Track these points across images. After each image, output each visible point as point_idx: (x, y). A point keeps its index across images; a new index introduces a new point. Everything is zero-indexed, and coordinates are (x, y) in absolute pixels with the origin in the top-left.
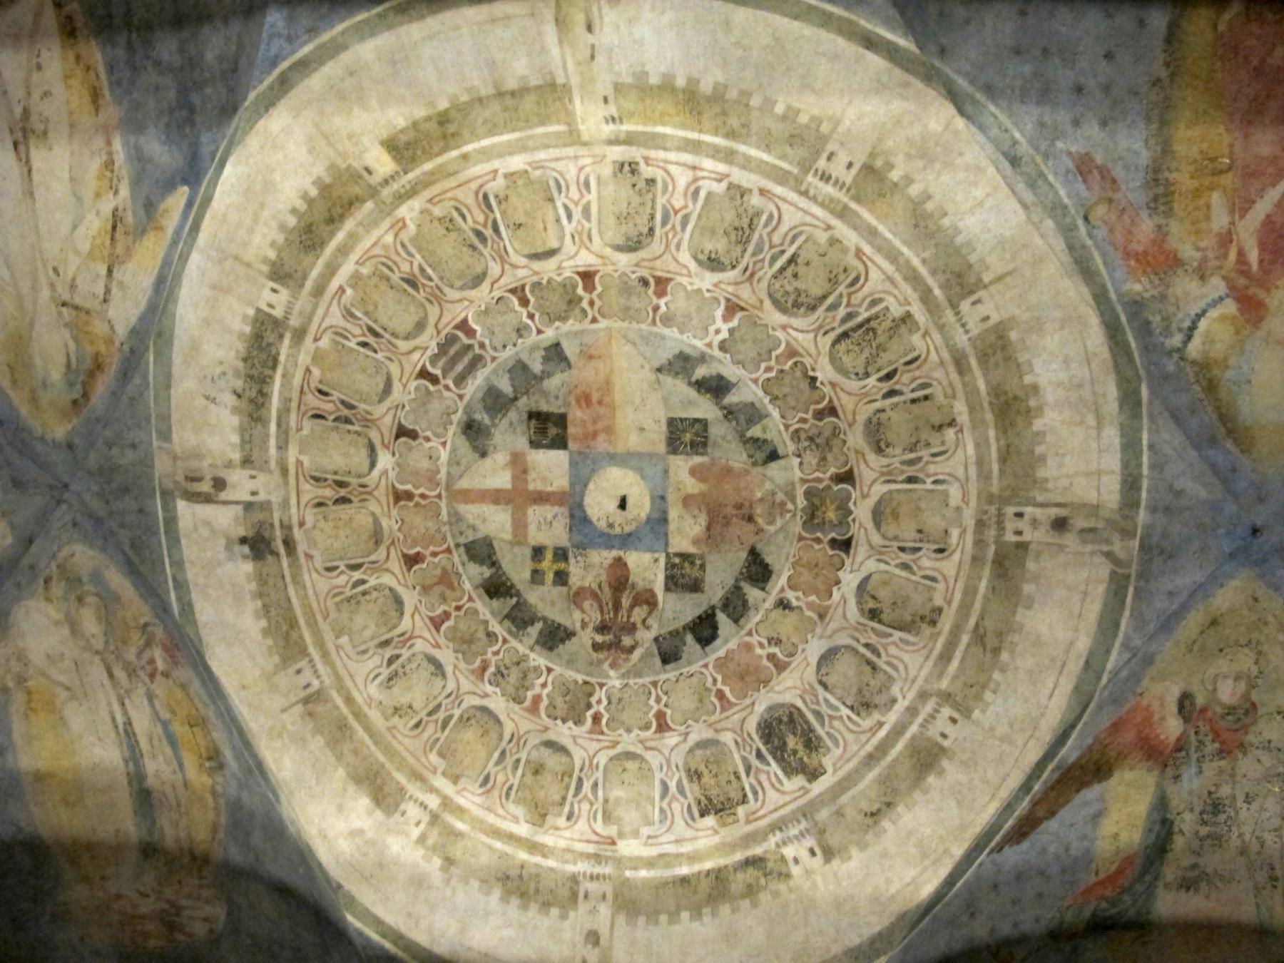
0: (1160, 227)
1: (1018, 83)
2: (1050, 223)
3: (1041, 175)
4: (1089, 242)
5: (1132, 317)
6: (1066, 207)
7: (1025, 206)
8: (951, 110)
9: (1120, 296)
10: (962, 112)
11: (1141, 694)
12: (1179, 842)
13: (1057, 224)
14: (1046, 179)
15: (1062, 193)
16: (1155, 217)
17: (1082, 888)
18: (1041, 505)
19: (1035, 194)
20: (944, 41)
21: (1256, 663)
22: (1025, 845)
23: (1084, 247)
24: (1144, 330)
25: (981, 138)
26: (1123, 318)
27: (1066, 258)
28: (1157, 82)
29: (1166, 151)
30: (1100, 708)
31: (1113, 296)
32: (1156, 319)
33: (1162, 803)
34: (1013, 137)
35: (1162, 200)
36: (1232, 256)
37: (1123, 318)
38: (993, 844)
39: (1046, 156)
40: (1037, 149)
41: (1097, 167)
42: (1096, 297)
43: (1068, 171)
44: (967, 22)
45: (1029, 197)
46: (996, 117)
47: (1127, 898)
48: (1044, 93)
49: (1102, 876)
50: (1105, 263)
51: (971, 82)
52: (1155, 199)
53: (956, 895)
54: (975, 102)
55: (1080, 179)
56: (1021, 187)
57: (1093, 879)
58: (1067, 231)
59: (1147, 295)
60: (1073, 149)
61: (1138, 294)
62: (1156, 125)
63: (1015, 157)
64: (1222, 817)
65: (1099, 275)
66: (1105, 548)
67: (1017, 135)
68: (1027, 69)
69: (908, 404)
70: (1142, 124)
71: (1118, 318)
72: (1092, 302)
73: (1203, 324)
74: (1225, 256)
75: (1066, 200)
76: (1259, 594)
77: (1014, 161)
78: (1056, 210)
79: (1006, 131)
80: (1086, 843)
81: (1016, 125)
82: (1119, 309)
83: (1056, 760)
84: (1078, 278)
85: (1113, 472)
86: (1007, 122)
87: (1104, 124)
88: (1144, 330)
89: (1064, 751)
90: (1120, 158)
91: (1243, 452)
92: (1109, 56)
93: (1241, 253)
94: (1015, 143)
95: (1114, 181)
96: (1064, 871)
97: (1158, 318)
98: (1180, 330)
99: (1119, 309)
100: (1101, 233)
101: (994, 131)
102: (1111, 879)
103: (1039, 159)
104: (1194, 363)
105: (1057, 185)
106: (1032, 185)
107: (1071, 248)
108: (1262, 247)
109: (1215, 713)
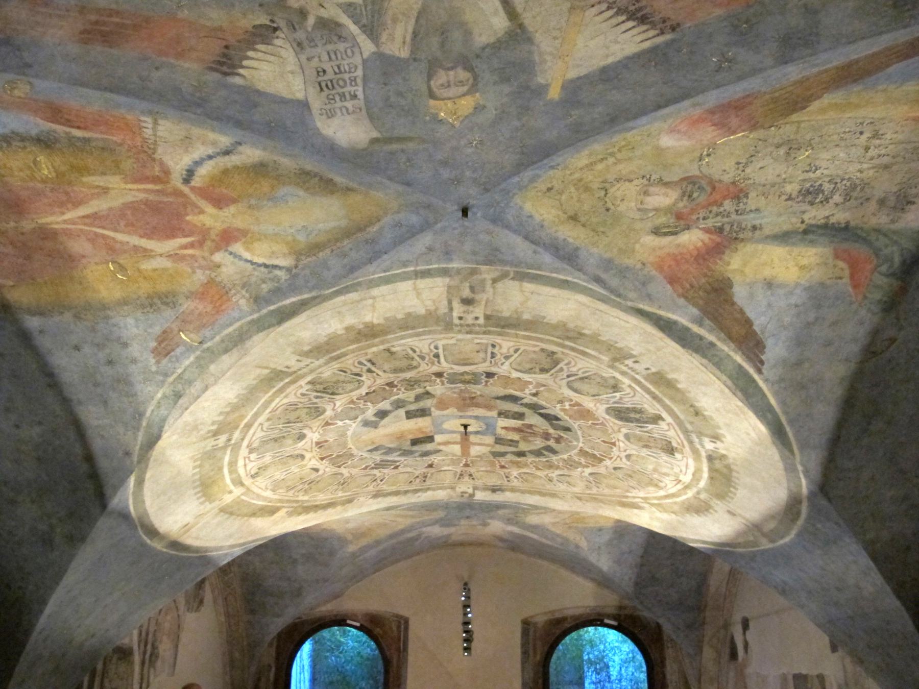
0: (187, 298)
1: (125, 399)
2: (212, 368)
3: (180, 377)
4: (218, 338)
5: (268, 302)
6: (197, 358)
7: (206, 388)
8: (161, 443)
9: (253, 312)
10: (158, 437)
11: (644, 264)
12: (840, 217)
13: (212, 362)
14: (182, 373)
15: (187, 362)
16: (180, 301)
17: (850, 289)
18: (451, 309)
19: (195, 380)
20: (120, 454)
21: (630, 181)
22: (769, 343)
23: (223, 341)
24: (278, 292)
25: (170, 420)
26: (272, 308)
27: (235, 353)
28: (77, 317)
29: (124, 302)
30: (649, 297)
31: (255, 316)
32: (265, 287)
33: (783, 238)
34: (162, 398)
35: (165, 300)
36: (190, 252)
37: (272, 308)
38: (751, 371)
39: (166, 375)
40: (163, 382)
41: (159, 344)
42: (260, 329)
43: (170, 361)
44: (103, 436)
45: (198, 385)
46: (153, 411)
47: (887, 251)
48: (123, 382)
49: (847, 273)
50: (231, 325)
51: (138, 430)
52: (167, 304)
53: (783, 403)
54: (149, 426)
55: (173, 353)
56: (193, 390)
57: (846, 280)
58: (213, 355)
59: (247, 295)
60: (153, 361)
61: (248, 300)
62: (109, 312)
63: (175, 395)
64: (827, 187)
65: (241, 327)
66: (489, 282)
67: (159, 395)
68: (113, 395)
69: (377, 364)
70: (113, 321)
71: (273, 311)
72: (265, 333)
73: (260, 260)
74: (192, 256)
75: (192, 359)
76: (544, 187)
77: (178, 396)
78: (201, 365)
79: (159, 403)
80: (798, 291)
81: (152, 398)
82: (265, 311)
83: (690, 325)
84: (249, 343)
85: (414, 284)
86: (154, 402)
87: (125, 345)
88: (278, 292)
89: (684, 321)
90: (146, 331)
91: (379, 220)
92: (77, 348)
93: (185, 247)
94: (165, 396)
95: (164, 332)
96: (819, 307)
97: (264, 286)
98: (270, 272)
99: (265, 311)
100: (207, 332)
101: (163, 411)
102: (854, 266)
103: (171, 379)
104: (298, 260)
105: (183, 367)
106: (190, 383)
107: (226, 351)
108: (173, 236)
109: (685, 207)
